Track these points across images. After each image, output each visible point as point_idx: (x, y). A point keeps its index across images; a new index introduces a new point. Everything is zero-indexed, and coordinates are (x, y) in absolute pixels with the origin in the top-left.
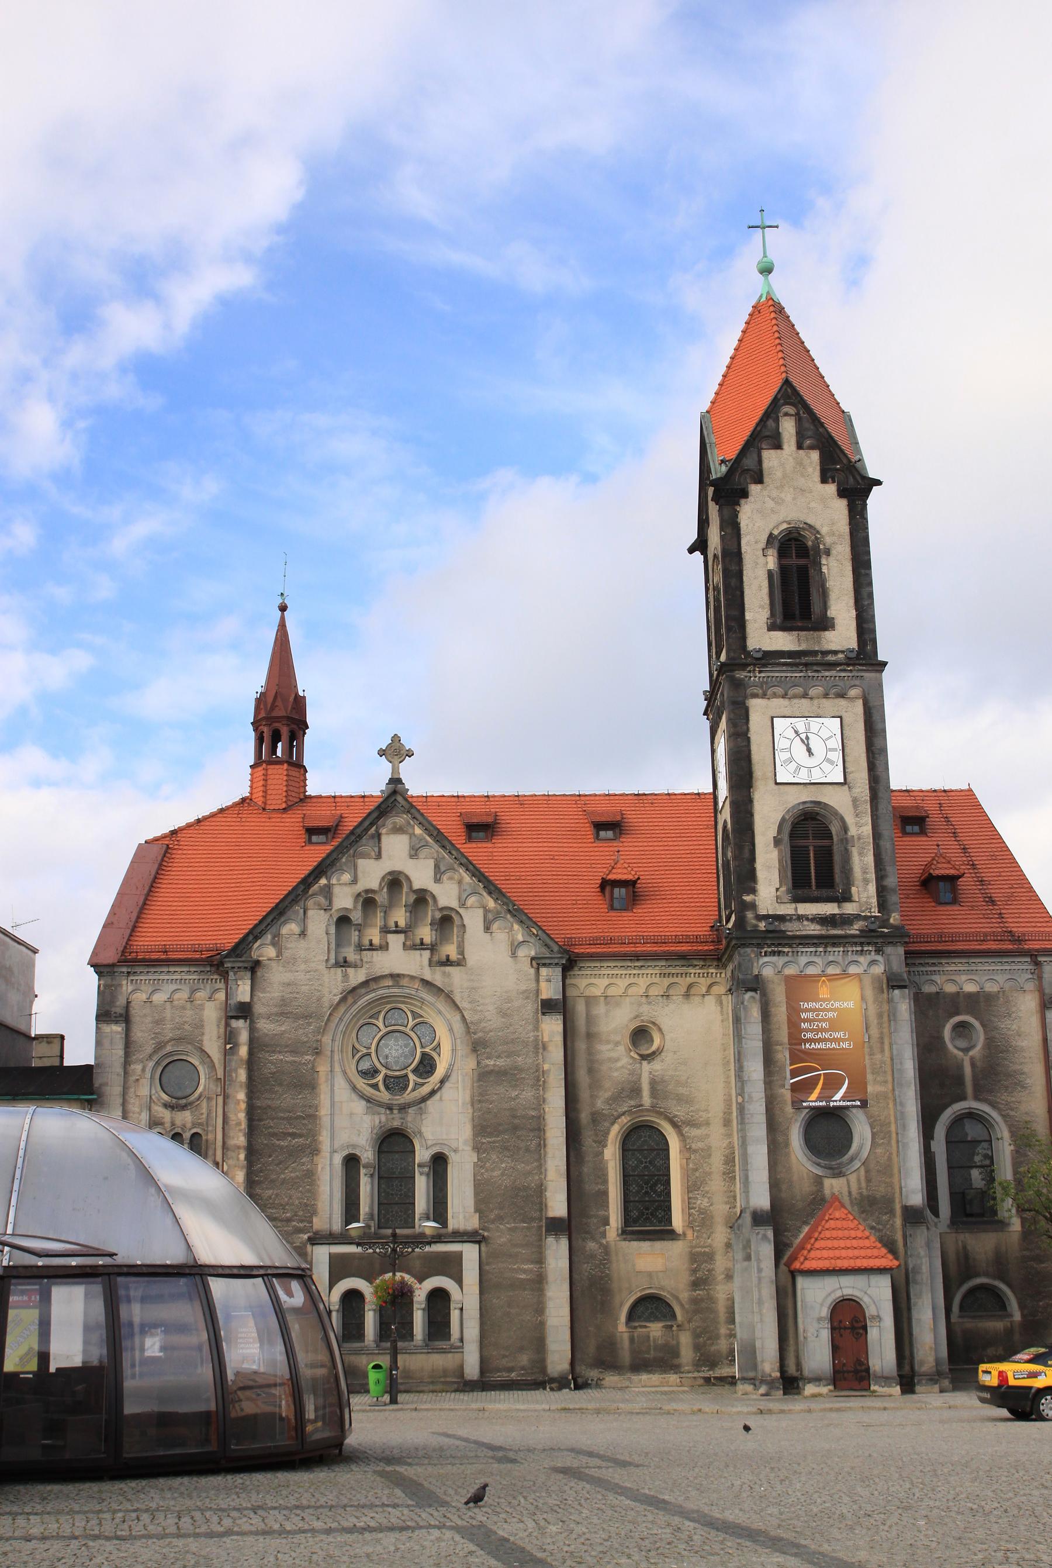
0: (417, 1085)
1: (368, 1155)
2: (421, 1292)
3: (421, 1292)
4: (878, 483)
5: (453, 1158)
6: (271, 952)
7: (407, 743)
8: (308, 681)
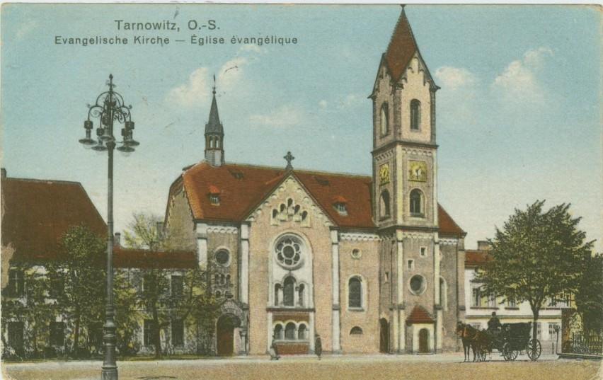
0: (295, 263)
1: (282, 285)
2: (298, 325)
3: (298, 325)
4: (440, 88)
5: (306, 287)
6: (252, 219)
7: (293, 154)
8: (223, 117)
